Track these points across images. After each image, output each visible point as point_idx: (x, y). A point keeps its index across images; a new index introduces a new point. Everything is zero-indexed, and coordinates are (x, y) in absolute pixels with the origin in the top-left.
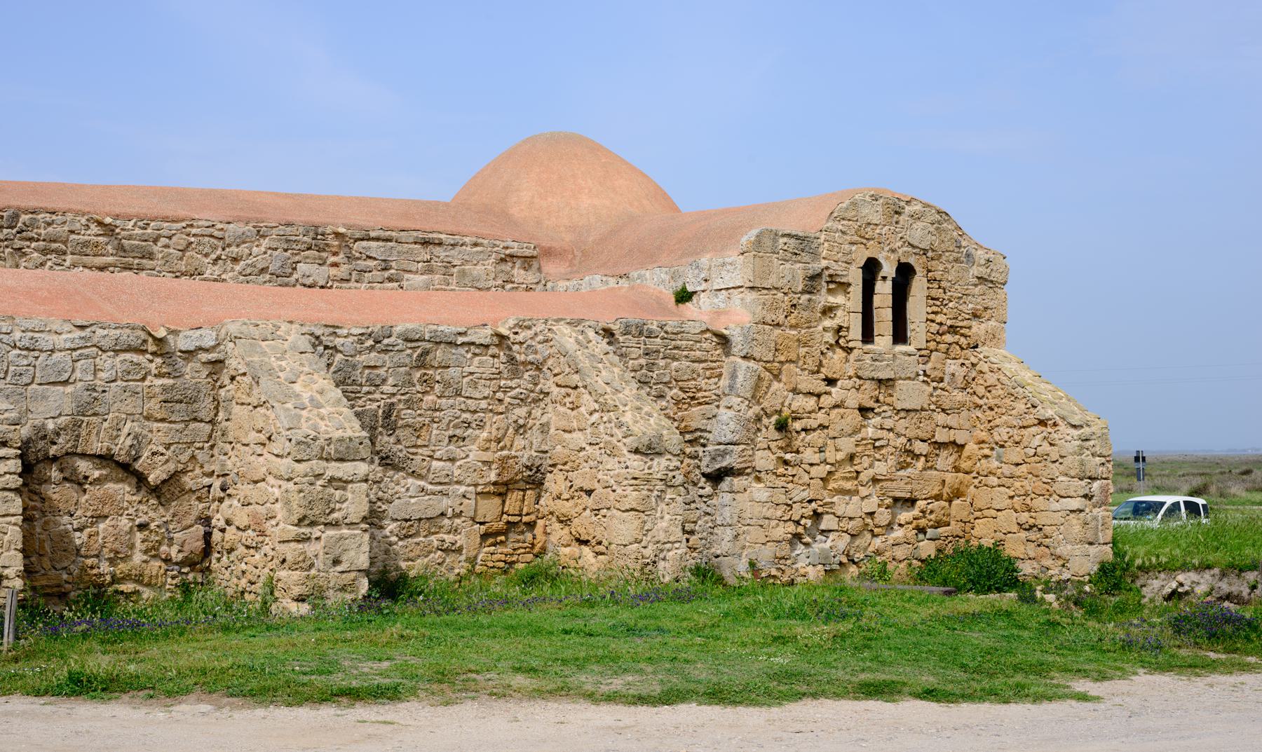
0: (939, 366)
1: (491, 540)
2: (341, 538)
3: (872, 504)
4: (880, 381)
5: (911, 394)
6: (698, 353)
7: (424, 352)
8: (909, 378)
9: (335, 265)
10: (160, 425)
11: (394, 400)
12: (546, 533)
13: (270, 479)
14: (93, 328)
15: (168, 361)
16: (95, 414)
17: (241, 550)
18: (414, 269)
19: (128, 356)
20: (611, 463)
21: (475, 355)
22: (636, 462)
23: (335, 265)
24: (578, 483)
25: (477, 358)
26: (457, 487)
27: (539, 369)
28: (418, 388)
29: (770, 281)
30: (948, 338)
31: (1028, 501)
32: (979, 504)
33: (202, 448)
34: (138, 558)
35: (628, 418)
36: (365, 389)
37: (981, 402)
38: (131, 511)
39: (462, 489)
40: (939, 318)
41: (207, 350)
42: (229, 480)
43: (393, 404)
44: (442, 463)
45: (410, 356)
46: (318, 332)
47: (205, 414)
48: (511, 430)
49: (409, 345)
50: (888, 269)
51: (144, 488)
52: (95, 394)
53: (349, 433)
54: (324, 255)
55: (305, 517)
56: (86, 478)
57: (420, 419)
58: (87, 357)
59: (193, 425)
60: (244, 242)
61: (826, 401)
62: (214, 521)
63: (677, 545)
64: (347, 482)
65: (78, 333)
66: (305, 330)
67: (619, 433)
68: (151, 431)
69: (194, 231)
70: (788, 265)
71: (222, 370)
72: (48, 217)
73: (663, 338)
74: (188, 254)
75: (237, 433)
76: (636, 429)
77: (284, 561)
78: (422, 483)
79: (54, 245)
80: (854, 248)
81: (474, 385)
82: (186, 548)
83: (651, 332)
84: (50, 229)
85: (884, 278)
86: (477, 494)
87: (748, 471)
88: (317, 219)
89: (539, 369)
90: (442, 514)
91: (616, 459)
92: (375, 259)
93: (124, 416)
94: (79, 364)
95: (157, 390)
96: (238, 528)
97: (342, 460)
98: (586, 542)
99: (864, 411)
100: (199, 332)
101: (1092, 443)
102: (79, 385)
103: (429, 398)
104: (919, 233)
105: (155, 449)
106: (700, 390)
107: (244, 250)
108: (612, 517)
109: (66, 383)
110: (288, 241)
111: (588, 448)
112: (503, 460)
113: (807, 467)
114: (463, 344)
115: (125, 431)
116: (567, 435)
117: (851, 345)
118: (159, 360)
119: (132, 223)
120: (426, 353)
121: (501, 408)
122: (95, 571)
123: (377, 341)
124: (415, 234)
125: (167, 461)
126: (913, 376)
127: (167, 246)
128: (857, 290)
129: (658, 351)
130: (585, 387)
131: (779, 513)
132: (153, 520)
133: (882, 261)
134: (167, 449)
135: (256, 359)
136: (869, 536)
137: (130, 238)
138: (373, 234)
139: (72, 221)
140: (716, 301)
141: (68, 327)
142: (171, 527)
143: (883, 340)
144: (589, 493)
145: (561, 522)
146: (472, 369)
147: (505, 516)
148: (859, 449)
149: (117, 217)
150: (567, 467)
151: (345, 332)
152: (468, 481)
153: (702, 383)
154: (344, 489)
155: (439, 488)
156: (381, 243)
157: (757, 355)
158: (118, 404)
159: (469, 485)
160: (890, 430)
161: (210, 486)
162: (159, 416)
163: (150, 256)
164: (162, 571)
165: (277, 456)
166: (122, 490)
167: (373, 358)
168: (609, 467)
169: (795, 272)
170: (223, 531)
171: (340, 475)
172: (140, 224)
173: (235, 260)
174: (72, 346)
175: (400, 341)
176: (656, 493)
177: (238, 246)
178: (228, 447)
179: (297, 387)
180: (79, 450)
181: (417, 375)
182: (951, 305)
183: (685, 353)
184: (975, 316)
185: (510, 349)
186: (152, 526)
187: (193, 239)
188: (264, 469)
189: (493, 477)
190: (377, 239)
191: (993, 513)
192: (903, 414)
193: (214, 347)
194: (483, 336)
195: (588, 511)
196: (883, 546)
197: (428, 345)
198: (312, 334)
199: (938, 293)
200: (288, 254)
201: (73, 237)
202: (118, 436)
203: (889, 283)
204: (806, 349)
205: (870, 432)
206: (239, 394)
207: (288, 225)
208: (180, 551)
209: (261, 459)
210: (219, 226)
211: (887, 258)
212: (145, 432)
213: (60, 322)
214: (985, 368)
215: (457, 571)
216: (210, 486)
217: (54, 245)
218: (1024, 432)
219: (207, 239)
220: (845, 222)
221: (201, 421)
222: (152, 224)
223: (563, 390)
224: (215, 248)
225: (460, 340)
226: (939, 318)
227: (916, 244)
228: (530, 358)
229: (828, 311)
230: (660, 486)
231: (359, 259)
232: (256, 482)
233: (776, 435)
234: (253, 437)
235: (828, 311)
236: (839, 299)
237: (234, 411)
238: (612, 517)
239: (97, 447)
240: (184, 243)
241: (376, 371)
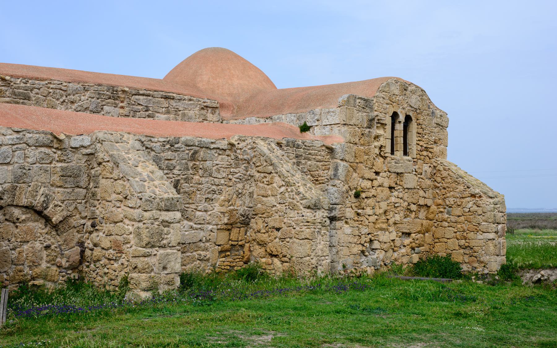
0: (421, 167)
1: (223, 255)
2: (168, 255)
3: (393, 236)
4: (398, 173)
5: (410, 181)
6: (319, 157)
7: (195, 152)
8: (409, 173)
9: (122, 107)
10: (59, 189)
11: (179, 178)
12: (250, 251)
13: (127, 221)
14: (24, 133)
15: (64, 153)
16: (24, 183)
17: (104, 261)
18: (161, 111)
19: (43, 149)
20: (293, 214)
21: (219, 154)
22: (308, 214)
23: (122, 107)
24: (271, 224)
25: (220, 156)
26: (208, 226)
27: (248, 163)
28: (191, 171)
29: (353, 121)
30: (425, 153)
31: (465, 234)
32: (437, 235)
33: (81, 203)
34: (44, 265)
35: (301, 189)
37: (439, 185)
38: (41, 238)
39: (210, 227)
40: (421, 143)
41: (85, 147)
42: (97, 221)
43: (179, 180)
44: (201, 213)
45: (188, 154)
46: (143, 140)
47: (82, 184)
48: (235, 196)
49: (188, 148)
50: (402, 118)
51: (49, 226)
52: (24, 171)
53: (171, 196)
54: (117, 102)
55: (149, 243)
56: (18, 219)
57: (192, 189)
58: (21, 149)
59: (77, 190)
60: (77, 94)
61: (376, 183)
62: (86, 245)
63: (327, 258)
64: (170, 223)
65: (15, 136)
66: (137, 138)
67: (298, 198)
68: (54, 193)
69: (52, 86)
70: (360, 114)
71: (92, 158)
73: (304, 149)
74: (48, 98)
75: (103, 195)
76: (307, 195)
77: (136, 267)
78: (191, 224)
80: (388, 106)
81: (218, 171)
82: (71, 260)
83: (298, 145)
85: (400, 122)
86: (218, 229)
87: (343, 218)
88: (113, 83)
89: (248, 163)
90: (200, 241)
91: (296, 212)
92: (142, 105)
93: (40, 184)
94: (16, 153)
95: (58, 169)
96: (103, 248)
97: (168, 210)
98: (276, 256)
99: (391, 188)
100: (81, 137)
101: (498, 206)
102: (16, 165)
103: (197, 177)
104: (414, 100)
105: (56, 203)
106: (320, 176)
107: (77, 97)
108: (293, 243)
109: (8, 164)
110: (99, 94)
111: (278, 205)
112: (231, 211)
113: (367, 216)
114: (214, 148)
115: (41, 192)
116: (264, 199)
117: (386, 155)
118: (59, 152)
119: (19, 80)
120: (196, 152)
121: (231, 184)
122: (22, 274)
123: (172, 144)
124: (161, 93)
125: (63, 210)
126: (411, 171)
127: (37, 94)
128: (389, 127)
129: (301, 156)
130: (277, 173)
131: (356, 240)
132: (53, 244)
133: (399, 113)
134: (63, 203)
135: (115, 153)
136: (391, 251)
137: (18, 88)
138: (141, 92)
140: (324, 131)
141: (10, 132)
142: (63, 248)
143: (399, 154)
144: (278, 229)
145: (260, 245)
146: (217, 162)
147: (230, 242)
148: (389, 208)
149: (12, 76)
150: (264, 216)
151: (156, 140)
152: (214, 222)
153: (321, 172)
154: (168, 226)
156: (145, 97)
157: (347, 159)
158: (38, 177)
159: (214, 225)
160: (401, 198)
161: (84, 225)
162: (59, 184)
163: (29, 98)
164: (57, 273)
165: (131, 208)
166: (38, 226)
167: (169, 155)
168: (291, 216)
169: (361, 117)
170: (92, 250)
171: (167, 219)
172: (24, 81)
173: (72, 102)
174: (13, 143)
175: (183, 146)
176: (317, 230)
177: (74, 95)
178: (96, 203)
179: (139, 169)
180: (15, 203)
181: (191, 164)
182: (426, 137)
183: (314, 157)
184: (435, 143)
185: (236, 152)
187: (51, 91)
188: (122, 216)
189: (226, 221)
190: (143, 95)
191: (445, 240)
192: (406, 190)
193: (89, 146)
194: (223, 144)
195: (277, 240)
196: (398, 257)
197: (197, 149)
198: (140, 140)
199: (420, 131)
200: (99, 101)
202: (36, 195)
203: (402, 125)
204: (367, 157)
205: (393, 199)
206: (105, 173)
207: (99, 85)
208: (67, 261)
209: (119, 210)
210: (65, 84)
211: (401, 112)
212: (51, 194)
213: (5, 129)
214: (441, 168)
215: (207, 271)
216: (84, 225)
218: (462, 200)
219: (58, 91)
220: (384, 93)
221: (81, 188)
222: (30, 81)
223: (262, 175)
224: (62, 96)
225: (212, 146)
226: (421, 143)
227: (413, 106)
228: (245, 157)
229: (377, 137)
230: (320, 227)
231: (133, 105)
232: (116, 223)
233: (354, 200)
234: (114, 196)
235: (377, 137)
236: (380, 132)
237: (101, 182)
238: (293, 243)
239: (24, 201)
240: (46, 92)
241: (171, 162)
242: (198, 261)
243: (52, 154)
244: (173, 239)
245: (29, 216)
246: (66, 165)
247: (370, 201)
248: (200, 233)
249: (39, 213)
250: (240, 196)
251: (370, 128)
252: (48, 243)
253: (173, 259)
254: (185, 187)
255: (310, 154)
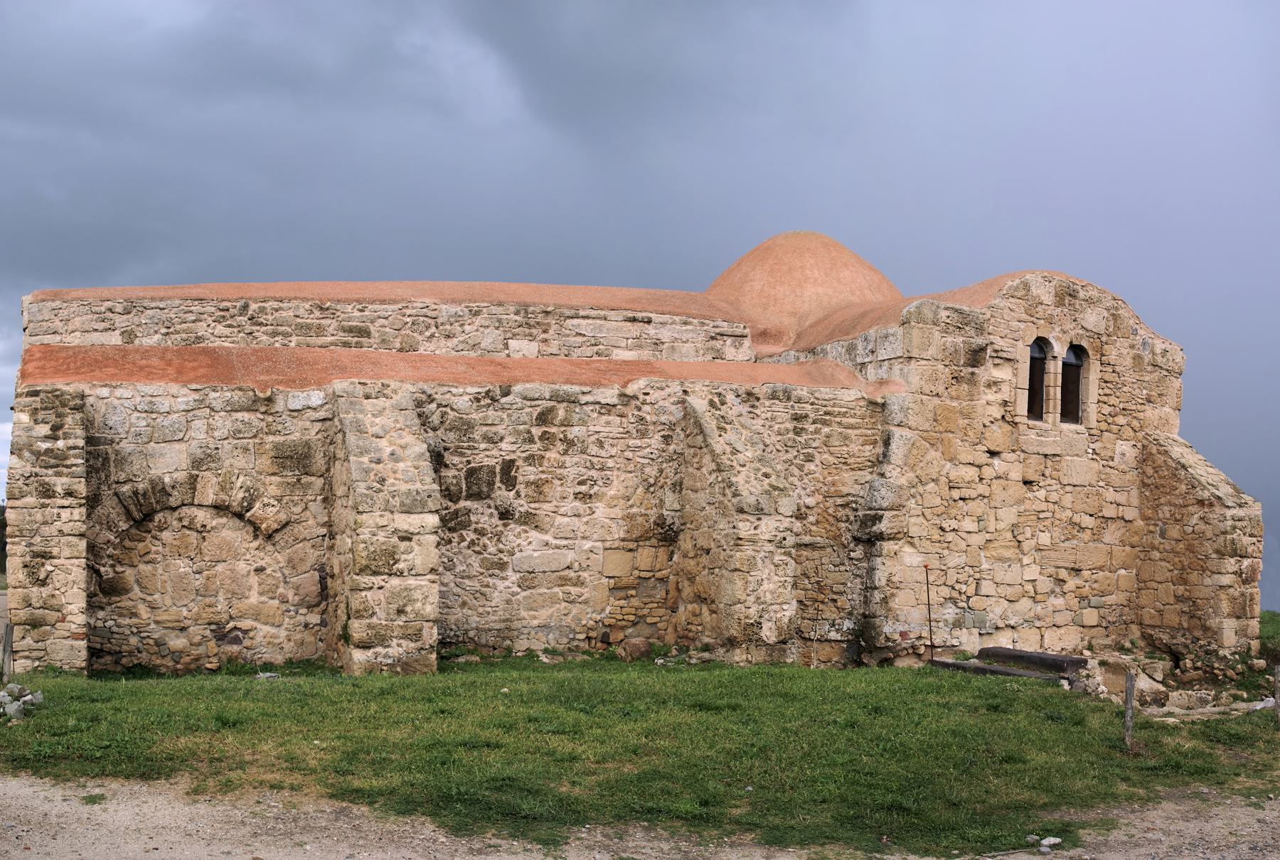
3: (1032, 572)
6: (852, 421)
10: (273, 478)
11: (512, 457)
19: (239, 415)
26: (585, 542)
29: (930, 352)
34: (254, 598)
36: (483, 446)
38: (248, 557)
39: (588, 545)
43: (513, 461)
44: (566, 519)
48: (640, 490)
55: (367, 567)
56: (204, 526)
57: (544, 476)
63: (785, 607)
69: (408, 312)
72: (276, 305)
73: (812, 404)
78: (548, 538)
79: (281, 329)
82: (301, 591)
84: (277, 315)
90: (568, 567)
106: (853, 456)
115: (239, 485)
122: (211, 610)
139: (298, 307)
144: (708, 551)
147: (636, 573)
152: (595, 536)
154: (410, 540)
155: (565, 542)
168: (721, 527)
176: (762, 554)
183: (838, 419)
186: (269, 571)
193: (322, 406)
201: (299, 320)
204: (966, 421)
215: (584, 622)
217: (281, 329)
220: (1011, 300)
238: (722, 576)
242: (564, 604)
243: (256, 423)
244: (418, 562)
245: (224, 520)
246: (282, 439)
247: (977, 507)
248: (565, 556)
249: (240, 516)
250: (652, 489)
251: (973, 366)
252: (262, 563)
253: (420, 597)
254: (527, 473)
255: (826, 413)
